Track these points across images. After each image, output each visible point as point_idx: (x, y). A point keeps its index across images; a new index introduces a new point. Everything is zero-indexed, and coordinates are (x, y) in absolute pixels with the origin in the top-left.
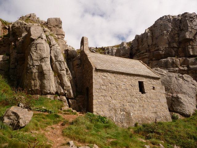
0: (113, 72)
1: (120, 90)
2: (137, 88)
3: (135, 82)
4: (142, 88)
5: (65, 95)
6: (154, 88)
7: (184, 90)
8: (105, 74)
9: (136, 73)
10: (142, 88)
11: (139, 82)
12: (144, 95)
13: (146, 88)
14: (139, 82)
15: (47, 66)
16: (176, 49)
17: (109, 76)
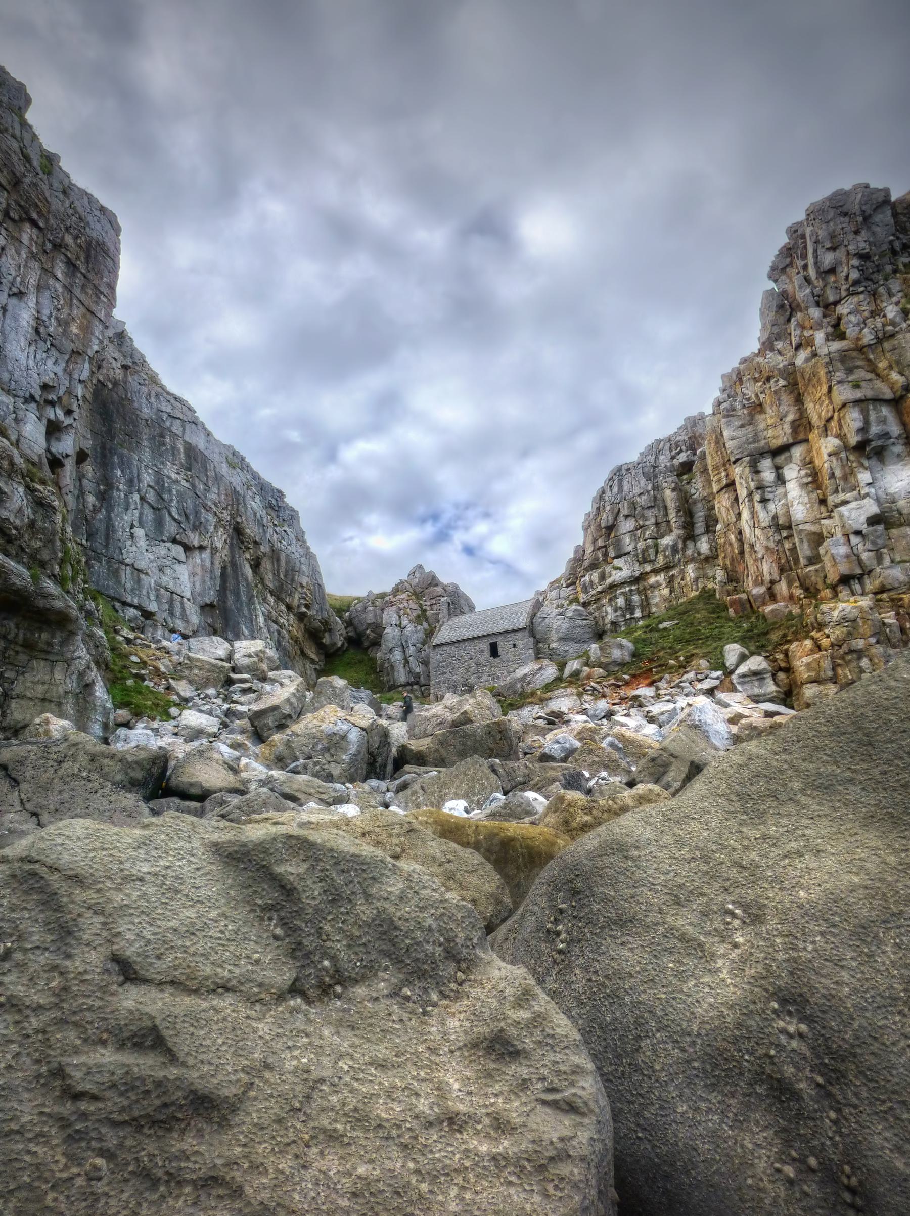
0: (453, 643)
1: (462, 661)
2: (487, 653)
3: (485, 646)
4: (494, 651)
5: (417, 683)
6: (514, 646)
7: (562, 635)
8: (445, 648)
9: (485, 633)
10: (494, 651)
11: (491, 644)
12: (497, 660)
13: (500, 649)
14: (491, 644)
15: (397, 656)
16: (604, 549)
17: (448, 648)
